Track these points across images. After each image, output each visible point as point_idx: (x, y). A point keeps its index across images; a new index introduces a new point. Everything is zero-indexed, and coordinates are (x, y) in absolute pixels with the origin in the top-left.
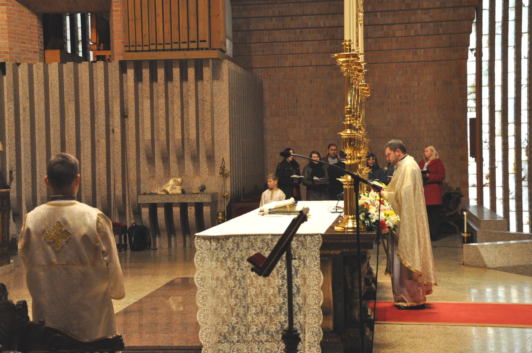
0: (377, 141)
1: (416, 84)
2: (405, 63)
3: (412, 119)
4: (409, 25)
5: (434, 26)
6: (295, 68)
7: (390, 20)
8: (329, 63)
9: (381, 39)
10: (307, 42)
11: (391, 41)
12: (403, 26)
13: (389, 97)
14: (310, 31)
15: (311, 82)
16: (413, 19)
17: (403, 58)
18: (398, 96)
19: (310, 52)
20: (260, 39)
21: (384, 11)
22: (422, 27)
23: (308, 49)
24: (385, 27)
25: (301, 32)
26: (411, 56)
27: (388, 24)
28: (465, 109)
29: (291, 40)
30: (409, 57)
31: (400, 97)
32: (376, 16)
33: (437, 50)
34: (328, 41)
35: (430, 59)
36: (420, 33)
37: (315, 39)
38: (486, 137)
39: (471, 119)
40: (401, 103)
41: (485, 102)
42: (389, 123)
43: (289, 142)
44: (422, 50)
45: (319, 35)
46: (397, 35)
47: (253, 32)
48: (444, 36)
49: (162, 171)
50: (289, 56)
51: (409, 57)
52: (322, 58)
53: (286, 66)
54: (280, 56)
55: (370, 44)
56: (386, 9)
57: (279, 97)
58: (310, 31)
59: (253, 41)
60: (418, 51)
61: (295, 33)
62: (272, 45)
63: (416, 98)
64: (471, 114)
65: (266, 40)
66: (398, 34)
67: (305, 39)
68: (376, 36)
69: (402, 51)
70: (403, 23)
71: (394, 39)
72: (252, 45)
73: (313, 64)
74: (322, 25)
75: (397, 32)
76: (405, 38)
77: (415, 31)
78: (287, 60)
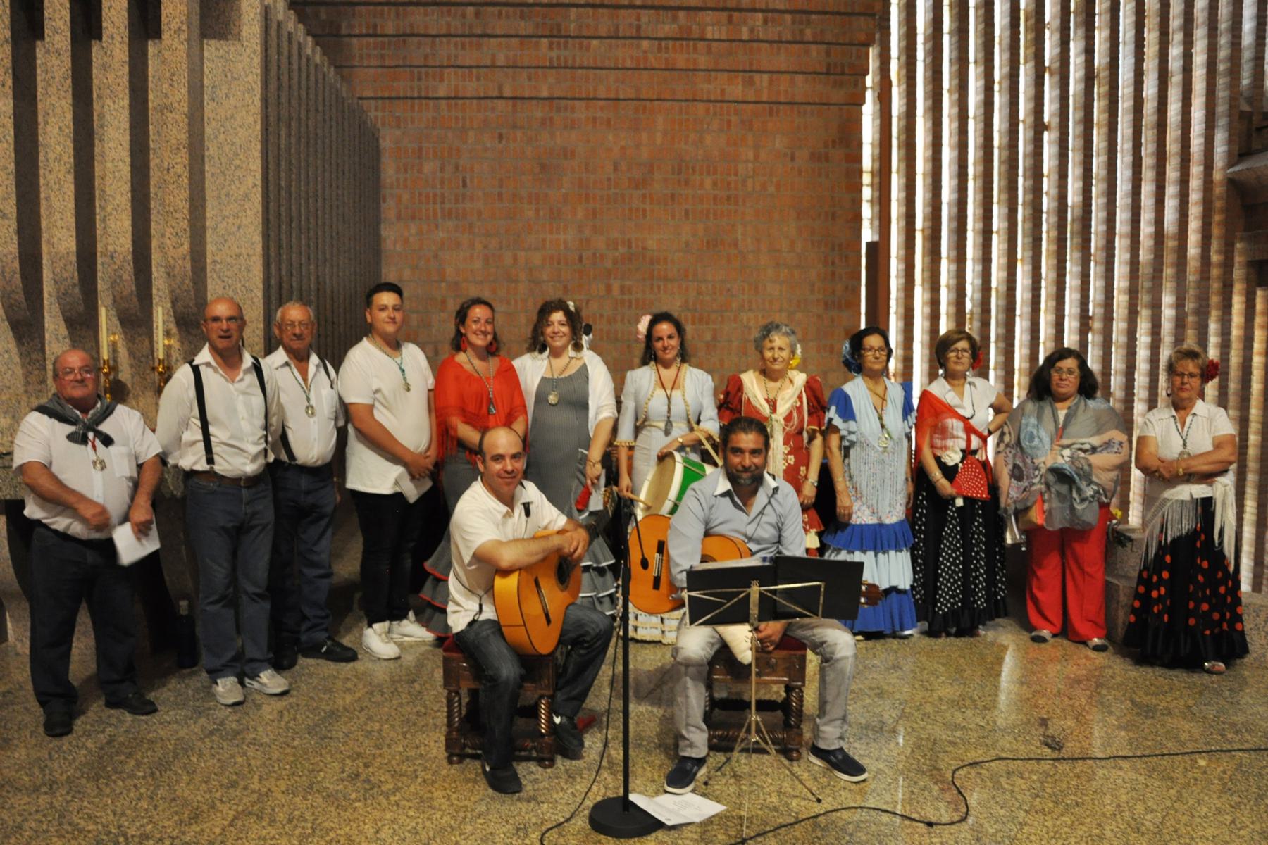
0: (659, 287)
1: (751, 155)
2: (725, 105)
3: (740, 237)
4: (736, 14)
5: (794, 22)
6: (460, 102)
8: (545, 94)
9: (671, 43)
10: (492, 40)
11: (695, 49)
12: (725, 14)
13: (687, 183)
14: (500, 13)
15: (501, 137)
17: (723, 91)
18: (708, 182)
19: (499, 64)
20: (375, 26)
22: (765, 21)
23: (493, 56)
24: (681, 14)
25: (477, 15)
26: (740, 87)
27: (688, 9)
29: (452, 32)
30: (736, 90)
31: (715, 184)
33: (799, 78)
34: (545, 41)
35: (782, 99)
36: (761, 36)
37: (513, 32)
38: (895, 283)
39: (870, 245)
40: (715, 198)
41: (896, 210)
42: (687, 243)
43: (443, 285)
44: (766, 76)
45: (522, 24)
46: (709, 36)
47: (358, 8)
48: (813, 47)
49: (19, 371)
50: (447, 71)
51: (736, 90)
52: (530, 79)
53: (441, 93)
54: (423, 70)
55: (645, 52)
57: (420, 171)
58: (500, 13)
59: (357, 31)
60: (757, 77)
61: (464, 16)
62: (404, 42)
63: (750, 189)
64: (868, 234)
65: (390, 29)
67: (489, 32)
68: (660, 35)
69: (719, 74)
70: (724, 9)
71: (701, 44)
72: (355, 40)
73: (507, 92)
75: (709, 28)
76: (726, 44)
77: (752, 31)
78: (442, 80)
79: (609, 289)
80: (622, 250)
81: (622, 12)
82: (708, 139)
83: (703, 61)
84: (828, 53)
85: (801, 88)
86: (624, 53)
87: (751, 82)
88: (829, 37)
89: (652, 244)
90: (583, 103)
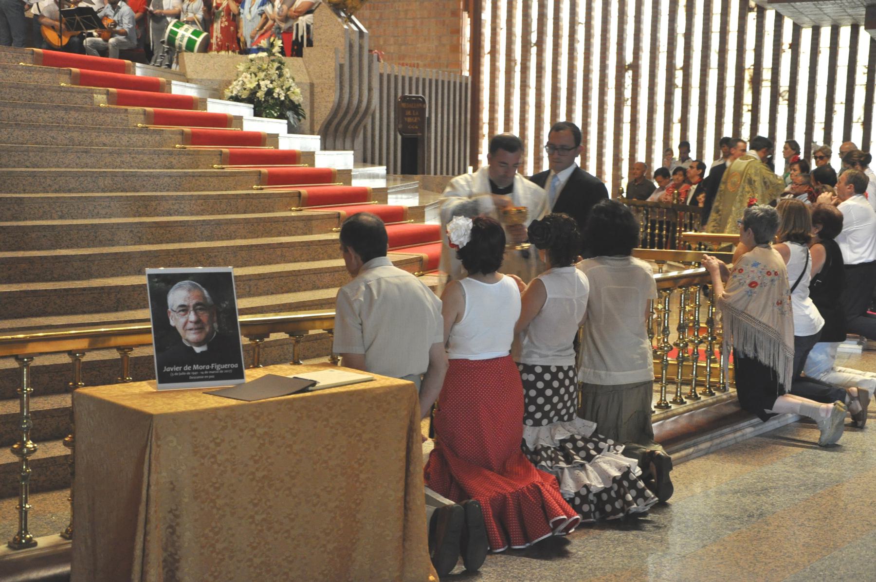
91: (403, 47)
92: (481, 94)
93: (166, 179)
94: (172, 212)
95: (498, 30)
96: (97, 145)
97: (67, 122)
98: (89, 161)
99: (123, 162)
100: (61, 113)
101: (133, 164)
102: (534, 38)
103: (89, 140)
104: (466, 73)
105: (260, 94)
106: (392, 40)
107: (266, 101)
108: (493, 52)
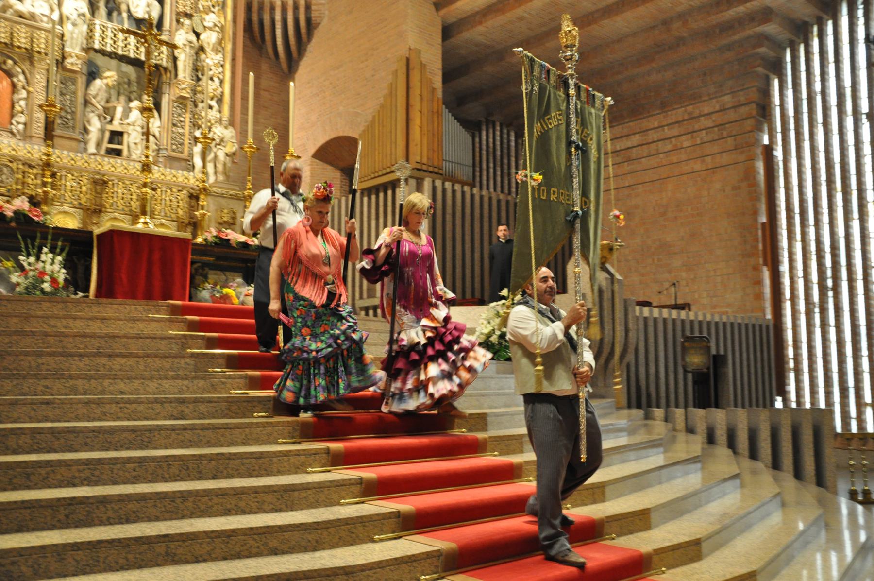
7: (675, 131)
16: (697, 127)
18: (689, 209)
21: (670, 124)
22: (707, 133)
24: (673, 140)
28: (756, 213)
30: (698, 166)
31: (692, 209)
32: (663, 130)
39: (763, 224)
51: (698, 166)
56: (670, 121)
66: (685, 144)
74: (618, 148)
77: (701, 139)
79: (653, 260)
80: (658, 243)
81: (651, 145)
82: (689, 190)
83: (683, 157)
84: (735, 140)
85: (725, 159)
86: (653, 162)
87: (703, 161)
88: (734, 133)
89: (668, 239)
90: (640, 186)
91: (714, 299)
92: (784, 333)
93: (126, 435)
94: (76, 481)
95: (796, 279)
96: (111, 394)
97: (111, 369)
98: (50, 414)
99: (105, 414)
100: (103, 360)
101: (120, 415)
102: (830, 283)
103: (100, 388)
104: (769, 316)
105: (494, 339)
106: (705, 294)
107: (500, 344)
108: (794, 298)
